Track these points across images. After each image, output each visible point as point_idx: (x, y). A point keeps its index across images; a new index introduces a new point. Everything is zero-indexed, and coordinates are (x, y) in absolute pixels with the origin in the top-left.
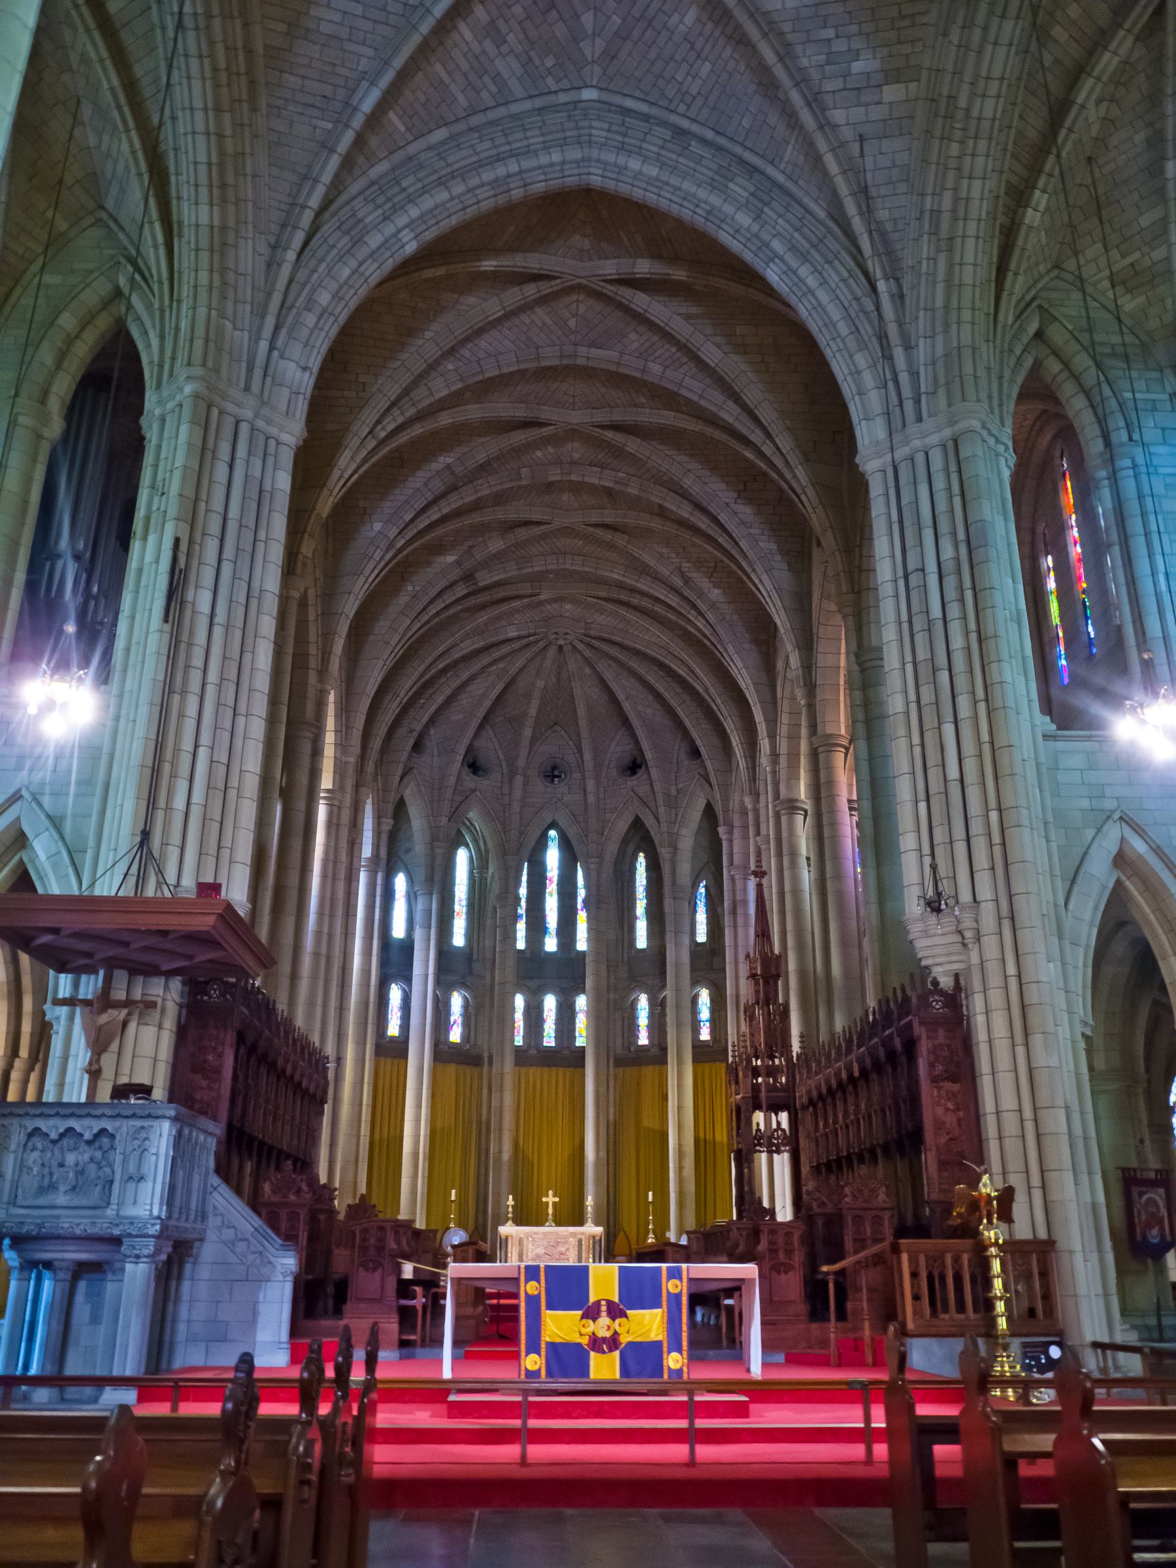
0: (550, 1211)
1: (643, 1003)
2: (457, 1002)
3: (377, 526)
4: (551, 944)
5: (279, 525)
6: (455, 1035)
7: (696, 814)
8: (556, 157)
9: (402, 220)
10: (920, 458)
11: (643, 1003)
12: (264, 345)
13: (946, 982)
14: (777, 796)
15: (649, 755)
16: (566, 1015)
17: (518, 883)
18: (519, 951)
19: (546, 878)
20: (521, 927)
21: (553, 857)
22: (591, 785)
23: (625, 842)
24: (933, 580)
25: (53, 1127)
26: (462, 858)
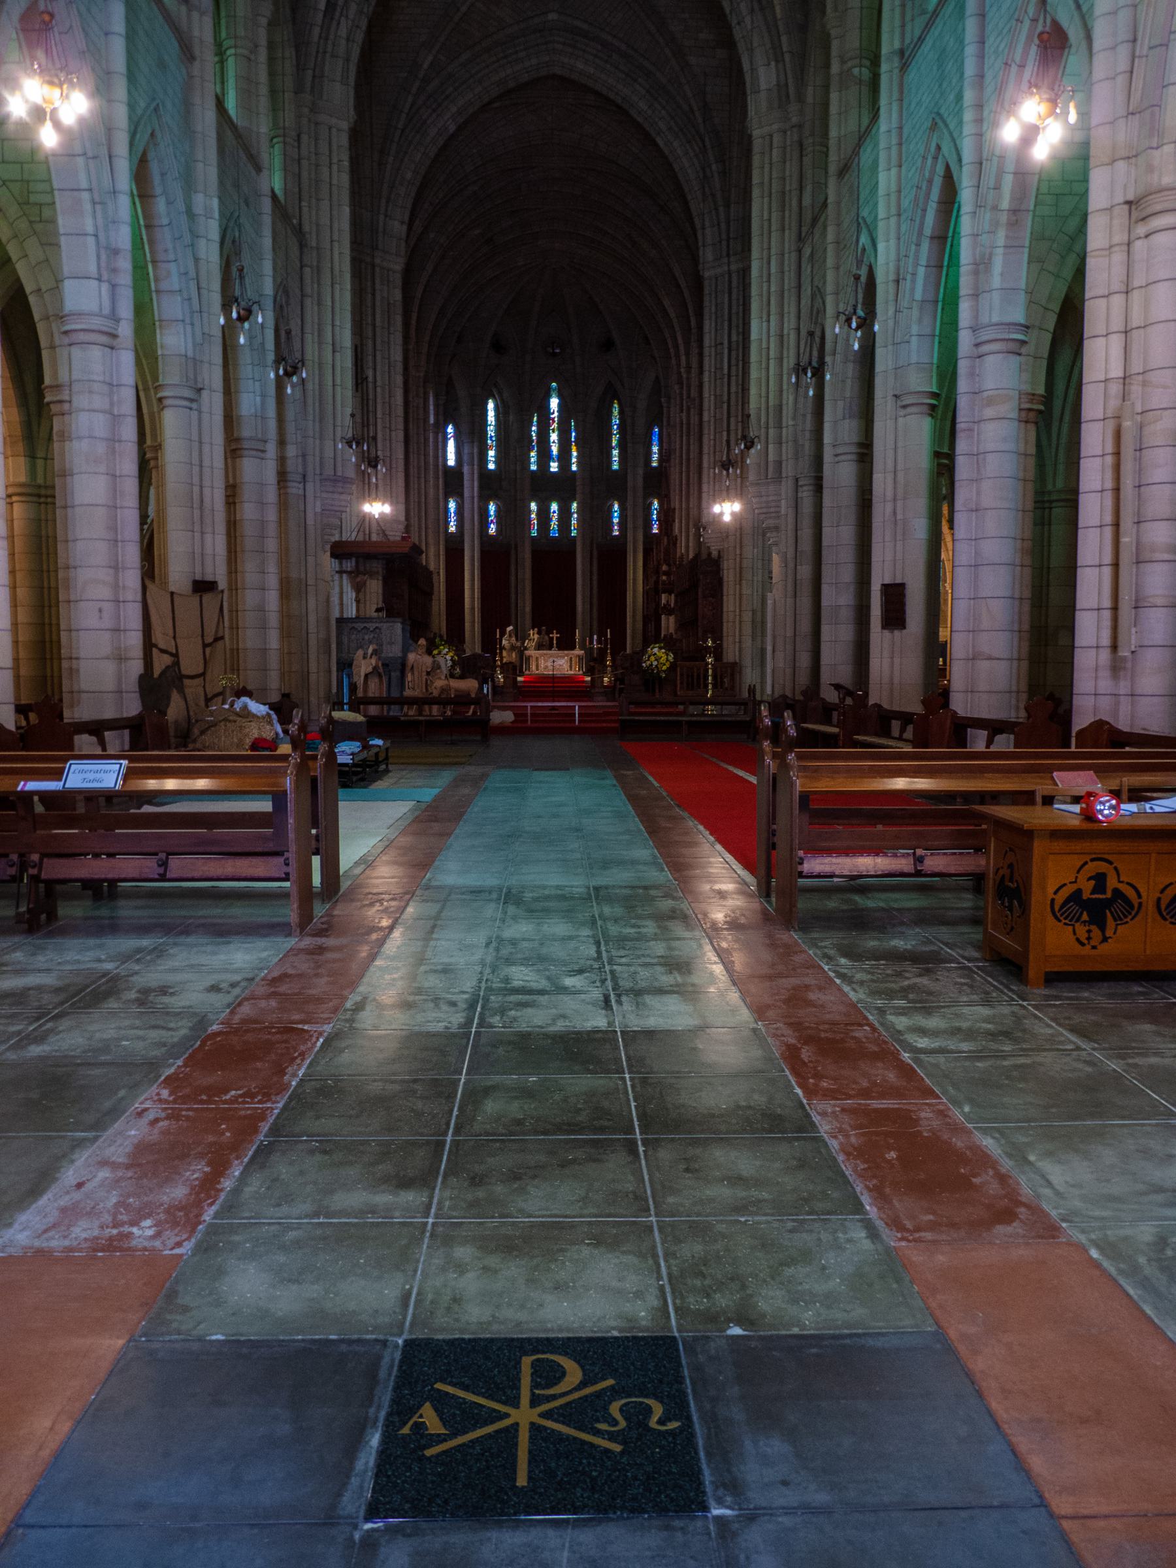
1: (616, 507)
2: (492, 508)
3: (432, 235)
4: (554, 467)
5: (399, 319)
6: (493, 529)
11: (616, 507)
12: (382, 217)
13: (715, 554)
14: (689, 397)
16: (565, 514)
18: (533, 471)
19: (549, 418)
21: (554, 403)
24: (726, 351)
25: (360, 626)
26: (491, 405)
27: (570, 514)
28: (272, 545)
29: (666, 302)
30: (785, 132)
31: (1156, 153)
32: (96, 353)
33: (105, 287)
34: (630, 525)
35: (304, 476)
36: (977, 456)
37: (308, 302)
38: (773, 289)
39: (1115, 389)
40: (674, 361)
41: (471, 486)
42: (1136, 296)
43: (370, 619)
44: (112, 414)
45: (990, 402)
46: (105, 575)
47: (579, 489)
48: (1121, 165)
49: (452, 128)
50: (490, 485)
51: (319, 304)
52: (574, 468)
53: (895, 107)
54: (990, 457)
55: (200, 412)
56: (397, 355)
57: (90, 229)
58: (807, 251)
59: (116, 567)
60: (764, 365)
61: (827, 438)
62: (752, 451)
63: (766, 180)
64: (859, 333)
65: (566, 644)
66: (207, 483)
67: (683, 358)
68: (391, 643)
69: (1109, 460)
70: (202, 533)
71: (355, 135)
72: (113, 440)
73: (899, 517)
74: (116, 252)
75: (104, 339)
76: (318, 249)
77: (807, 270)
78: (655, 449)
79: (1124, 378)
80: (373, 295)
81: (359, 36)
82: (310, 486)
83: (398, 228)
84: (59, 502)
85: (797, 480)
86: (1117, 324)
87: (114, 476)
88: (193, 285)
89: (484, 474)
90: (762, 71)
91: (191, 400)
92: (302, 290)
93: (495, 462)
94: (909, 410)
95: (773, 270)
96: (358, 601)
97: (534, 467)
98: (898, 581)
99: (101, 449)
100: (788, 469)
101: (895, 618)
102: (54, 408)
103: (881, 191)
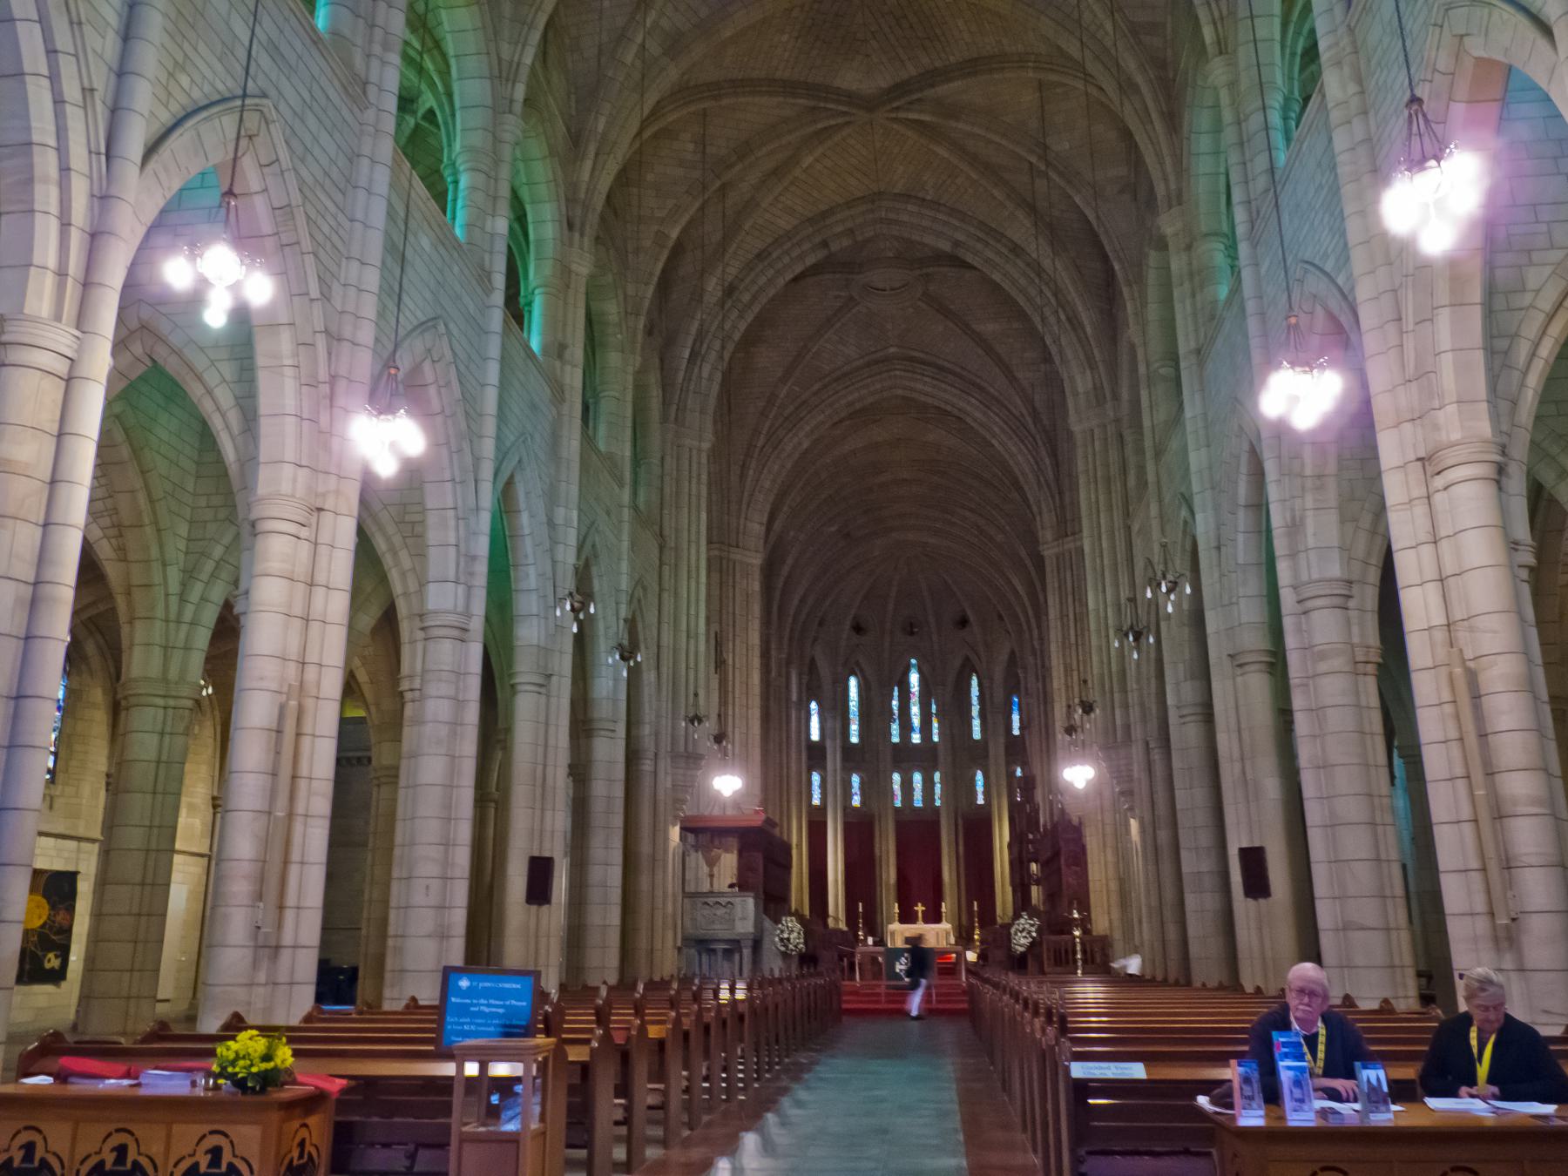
0: (920, 915)
1: (979, 777)
4: (916, 738)
5: (756, 609)
6: (856, 801)
7: (1004, 657)
8: (878, 386)
9: (801, 434)
10: (1067, 554)
11: (979, 777)
13: (1075, 821)
15: (972, 618)
16: (928, 785)
17: (891, 698)
18: (895, 744)
20: (895, 728)
21: (914, 678)
22: (935, 637)
23: (963, 666)
25: (711, 900)
27: (933, 784)
28: (618, 821)
29: (1016, 582)
30: (1105, 426)
31: (1440, 413)
32: (447, 646)
33: (461, 589)
34: (994, 795)
35: (656, 754)
36: (1317, 711)
37: (665, 595)
38: (1106, 562)
39: (1440, 636)
40: (1027, 635)
41: (834, 759)
42: (1444, 545)
43: (721, 894)
44: (455, 699)
45: (1322, 656)
46: (435, 852)
47: (941, 758)
48: (1407, 427)
49: (806, 445)
50: (852, 757)
51: (676, 594)
52: (936, 739)
53: (1197, 396)
54: (1330, 711)
55: (548, 696)
56: (755, 638)
57: (452, 540)
58: (1135, 527)
59: (447, 844)
60: (1103, 634)
61: (1171, 700)
62: (1092, 715)
63: (1091, 466)
64: (1172, 597)
65: (934, 916)
66: (550, 762)
67: (1035, 632)
68: (743, 919)
69: (1448, 709)
70: (543, 810)
71: (715, 454)
72: (456, 724)
73: (1249, 776)
74: (474, 558)
75: (455, 633)
76: (677, 549)
77: (1138, 543)
78: (1016, 718)
79: (1448, 625)
80: (734, 587)
81: (718, 376)
82: (662, 764)
83: (756, 528)
84: (402, 782)
85: (1147, 744)
86: (1430, 573)
87: (453, 757)
88: (549, 585)
89: (847, 748)
90: (1078, 379)
91: (541, 686)
92: (660, 585)
93: (861, 736)
94: (1247, 668)
95: (1105, 544)
96: (712, 876)
97: (896, 739)
98: (1257, 844)
99: (444, 731)
100: (1137, 732)
101: (1257, 885)
102: (408, 696)
103: (1193, 468)
